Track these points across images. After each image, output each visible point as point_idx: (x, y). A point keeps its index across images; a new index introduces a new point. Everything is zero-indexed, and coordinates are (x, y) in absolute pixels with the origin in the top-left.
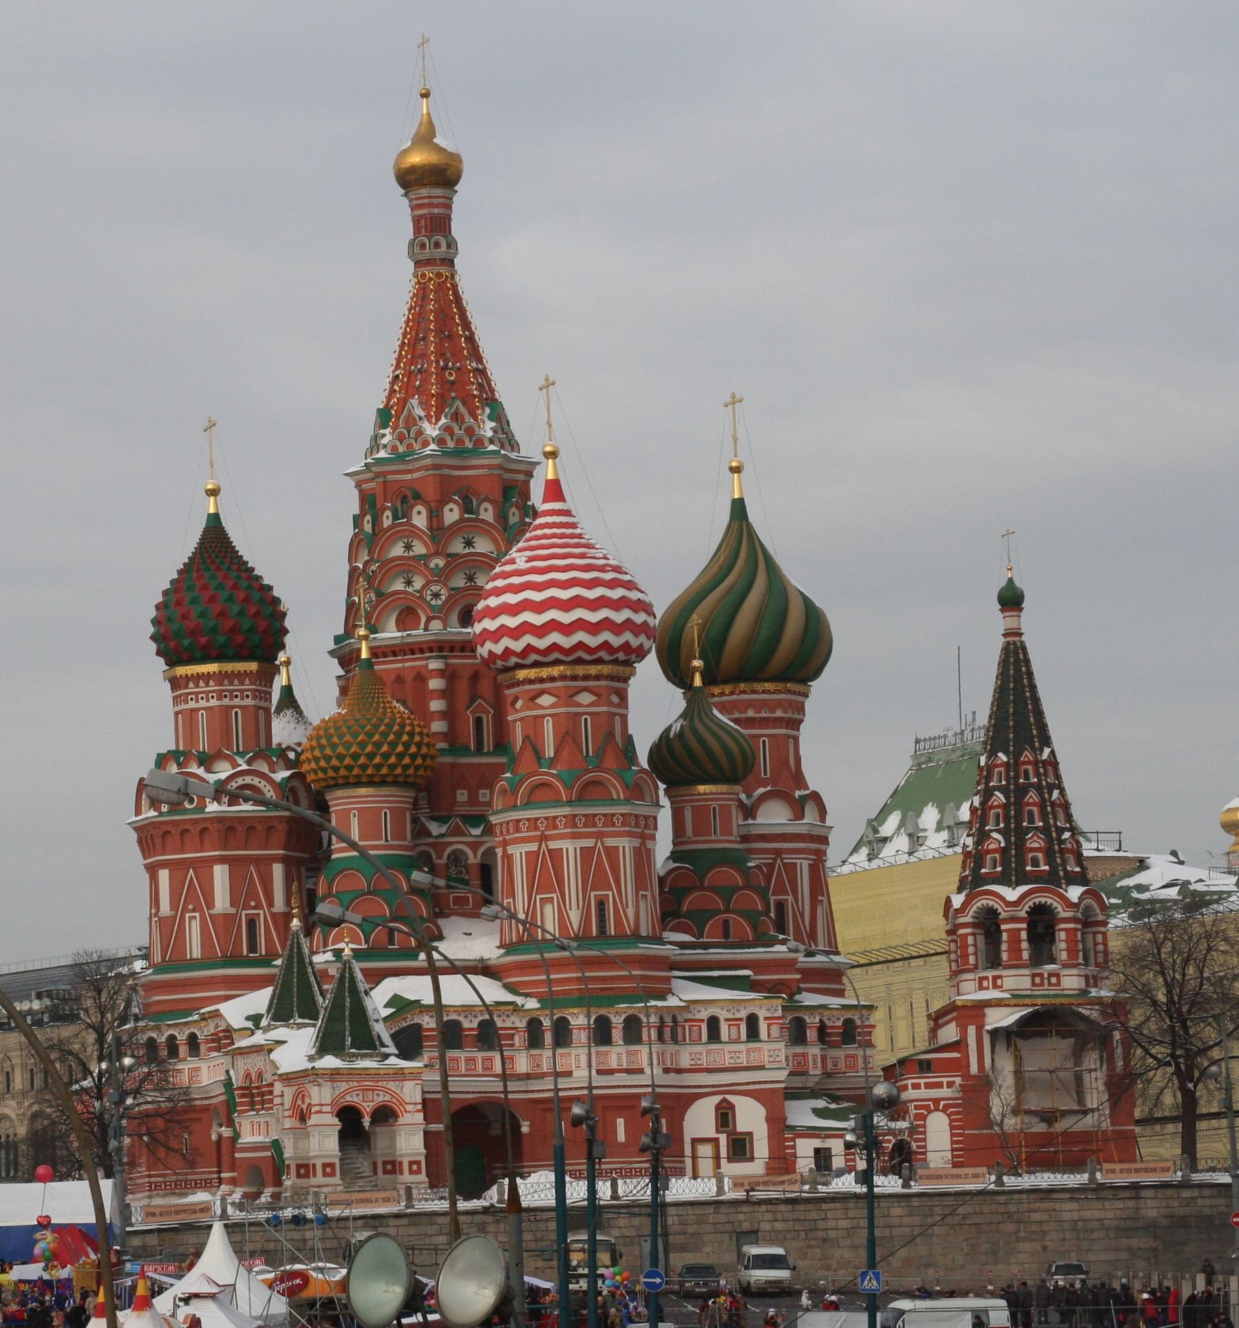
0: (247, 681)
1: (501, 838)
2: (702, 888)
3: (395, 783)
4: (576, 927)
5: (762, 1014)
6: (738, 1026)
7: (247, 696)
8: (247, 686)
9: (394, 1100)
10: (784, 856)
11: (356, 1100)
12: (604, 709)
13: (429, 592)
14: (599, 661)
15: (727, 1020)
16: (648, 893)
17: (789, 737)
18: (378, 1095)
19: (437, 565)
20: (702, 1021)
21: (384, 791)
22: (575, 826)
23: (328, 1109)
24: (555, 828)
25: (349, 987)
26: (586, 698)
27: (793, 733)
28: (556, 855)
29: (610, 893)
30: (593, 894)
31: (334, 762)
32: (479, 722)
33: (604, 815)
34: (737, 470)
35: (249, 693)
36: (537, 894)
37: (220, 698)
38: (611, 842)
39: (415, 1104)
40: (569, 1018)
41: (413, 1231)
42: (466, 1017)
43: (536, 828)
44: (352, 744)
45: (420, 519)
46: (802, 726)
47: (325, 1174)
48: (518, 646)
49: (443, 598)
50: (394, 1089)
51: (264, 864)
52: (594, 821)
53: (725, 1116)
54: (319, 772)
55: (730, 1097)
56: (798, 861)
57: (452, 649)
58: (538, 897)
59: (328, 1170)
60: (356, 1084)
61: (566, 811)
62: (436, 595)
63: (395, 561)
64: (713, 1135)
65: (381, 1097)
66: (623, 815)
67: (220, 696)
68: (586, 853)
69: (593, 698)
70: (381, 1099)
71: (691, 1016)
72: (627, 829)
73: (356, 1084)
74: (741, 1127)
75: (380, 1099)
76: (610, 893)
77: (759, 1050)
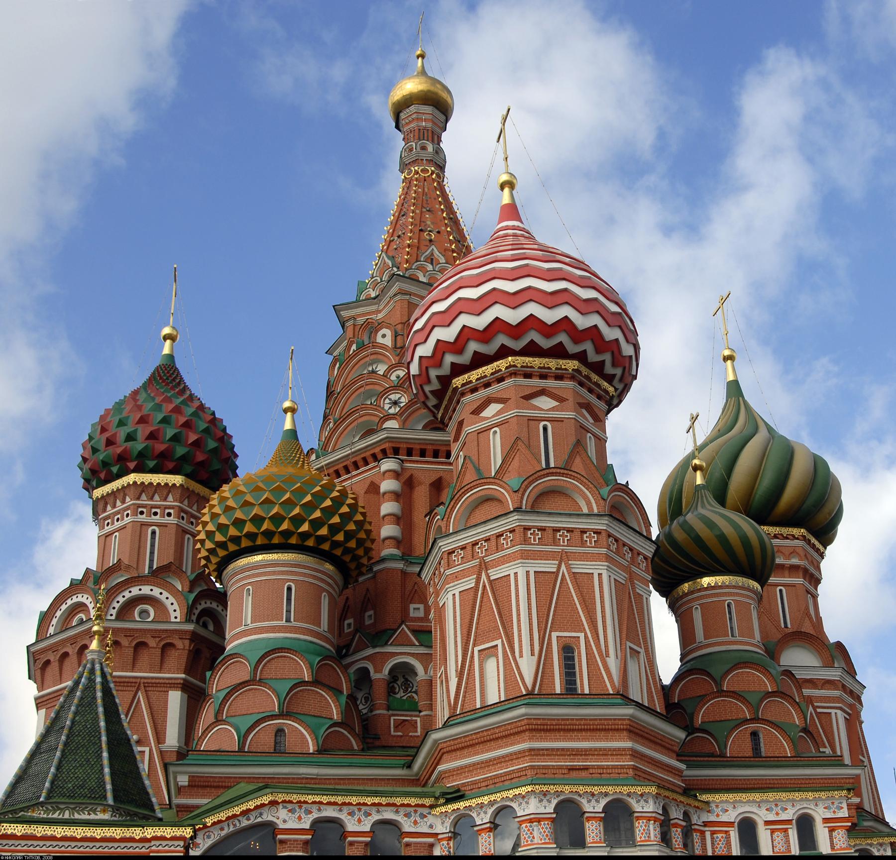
0: (170, 498)
2: (721, 693)
3: (299, 548)
4: (529, 681)
5: (819, 814)
6: (786, 830)
8: (171, 501)
10: (816, 704)
12: (570, 414)
14: (558, 352)
15: (767, 823)
16: (642, 651)
17: (808, 592)
20: (730, 824)
22: (526, 541)
25: (103, 699)
26: (544, 403)
27: (812, 589)
28: (500, 587)
29: (582, 635)
30: (554, 635)
31: (233, 531)
33: (570, 531)
34: (731, 358)
35: (172, 511)
36: (474, 645)
38: (580, 567)
40: (514, 805)
46: (820, 587)
48: (448, 334)
52: (554, 537)
54: (218, 549)
56: (833, 711)
57: (410, 453)
58: (476, 649)
61: (513, 521)
63: (354, 383)
66: (597, 532)
67: (137, 510)
69: (554, 403)
71: (712, 818)
72: (604, 551)
76: (582, 635)
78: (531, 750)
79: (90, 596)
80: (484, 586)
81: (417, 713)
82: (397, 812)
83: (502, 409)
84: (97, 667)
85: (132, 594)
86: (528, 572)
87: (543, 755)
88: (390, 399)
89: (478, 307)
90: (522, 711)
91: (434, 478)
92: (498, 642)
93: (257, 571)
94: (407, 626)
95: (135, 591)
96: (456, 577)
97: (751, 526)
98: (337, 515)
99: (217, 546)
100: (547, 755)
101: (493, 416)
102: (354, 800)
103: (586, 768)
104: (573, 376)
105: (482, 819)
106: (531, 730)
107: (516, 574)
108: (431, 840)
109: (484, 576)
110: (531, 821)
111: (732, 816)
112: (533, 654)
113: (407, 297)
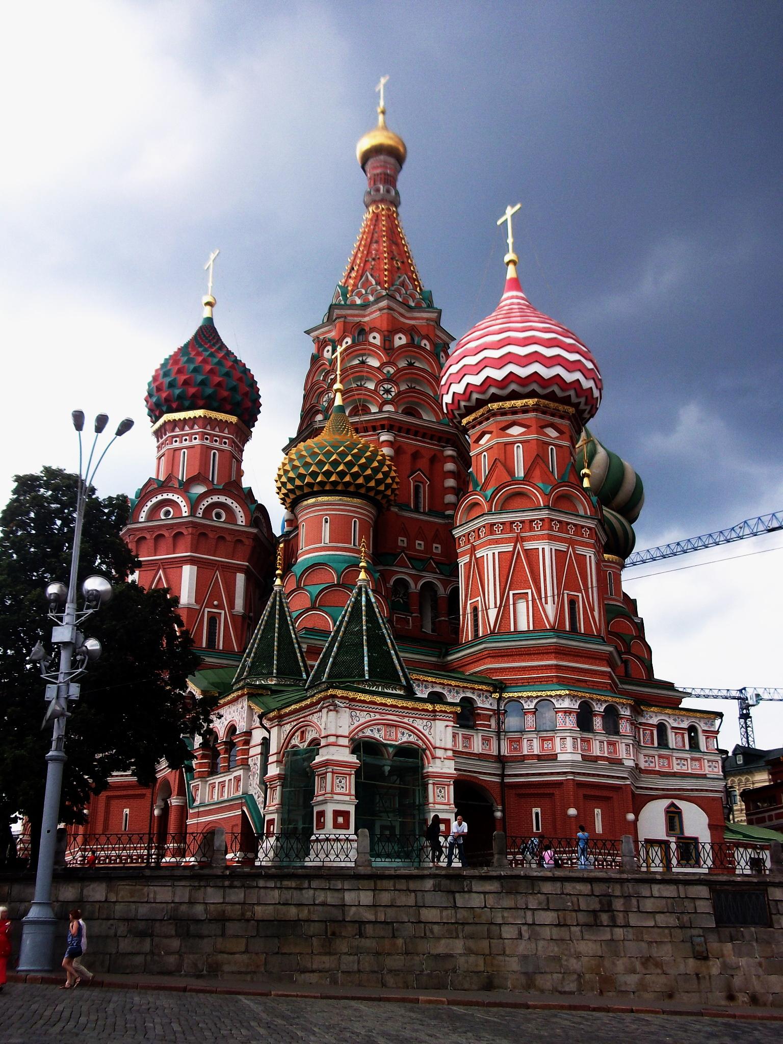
1: (469, 546)
4: (552, 619)
7: (225, 443)
9: (420, 742)
11: (377, 736)
13: (382, 388)
18: (403, 734)
19: (388, 372)
20: (652, 725)
21: (356, 501)
22: (551, 529)
23: (345, 742)
24: (531, 529)
29: (580, 595)
32: (417, 488)
37: (202, 439)
39: (446, 749)
41: (508, 902)
42: (450, 691)
43: (512, 531)
44: (318, 474)
45: (376, 339)
47: (336, 826)
49: (393, 394)
50: (421, 728)
51: (229, 571)
53: (674, 818)
55: (676, 802)
58: (511, 593)
59: (340, 820)
60: (378, 716)
61: (544, 514)
62: (388, 391)
64: (664, 837)
65: (406, 736)
68: (560, 556)
70: (404, 738)
73: (378, 716)
74: (689, 832)
75: (405, 739)
77: (698, 760)
78: (556, 665)
79: (201, 502)
80: (519, 552)
81: (410, 614)
82: (473, 693)
83: (524, 432)
84: (363, 589)
85: (213, 501)
86: (551, 549)
87: (563, 669)
88: (384, 388)
89: (525, 361)
90: (554, 640)
91: (413, 451)
92: (529, 591)
93: (333, 507)
94: (406, 554)
95: (215, 499)
96: (497, 542)
97: (620, 524)
98: (389, 478)
99: (288, 481)
100: (565, 670)
101: (518, 435)
102: (453, 683)
103: (586, 681)
104: (536, 408)
105: (529, 706)
106: (555, 653)
107: (543, 549)
108: (492, 713)
109: (518, 545)
110: (565, 712)
111: (654, 721)
112: (554, 603)
113: (392, 312)
